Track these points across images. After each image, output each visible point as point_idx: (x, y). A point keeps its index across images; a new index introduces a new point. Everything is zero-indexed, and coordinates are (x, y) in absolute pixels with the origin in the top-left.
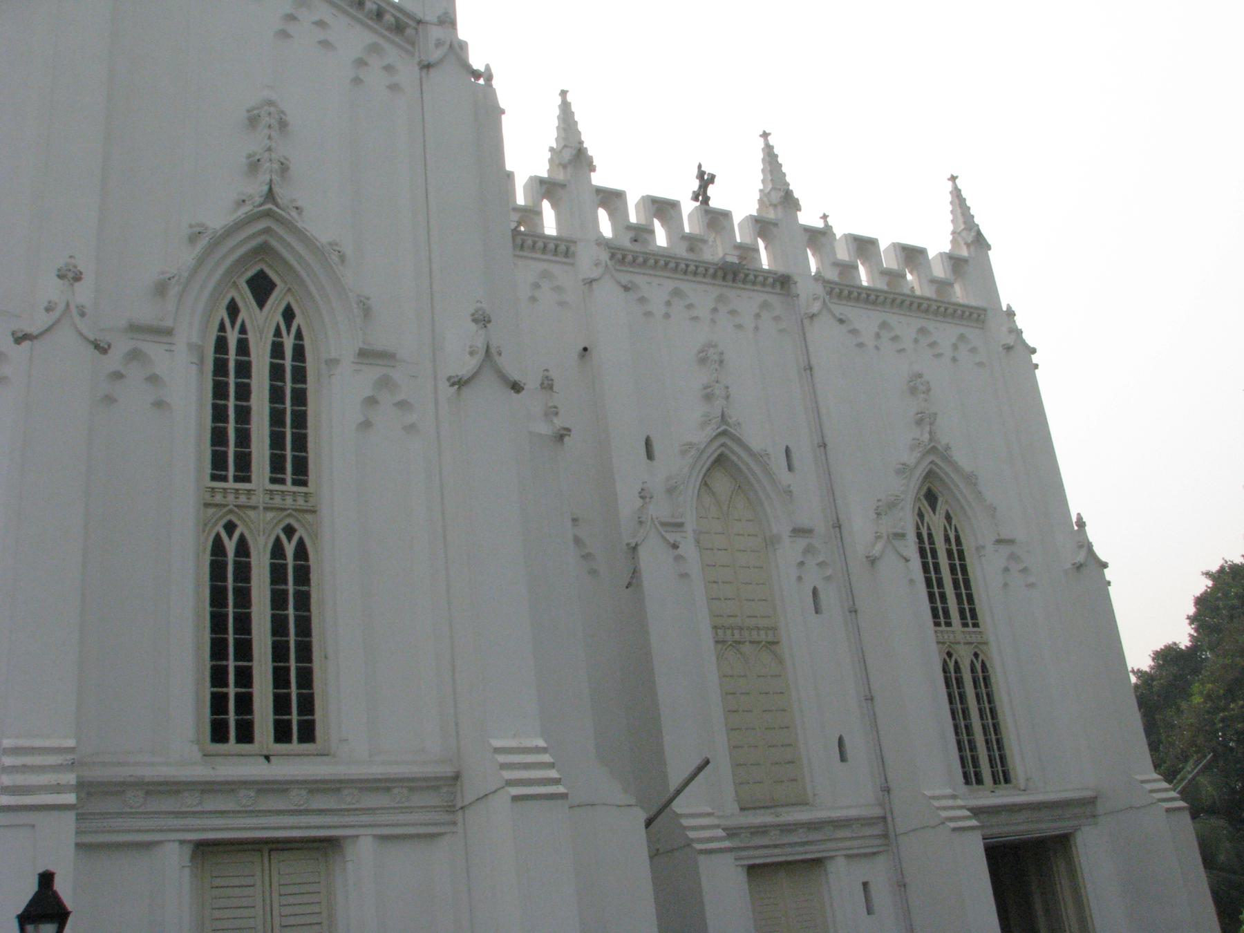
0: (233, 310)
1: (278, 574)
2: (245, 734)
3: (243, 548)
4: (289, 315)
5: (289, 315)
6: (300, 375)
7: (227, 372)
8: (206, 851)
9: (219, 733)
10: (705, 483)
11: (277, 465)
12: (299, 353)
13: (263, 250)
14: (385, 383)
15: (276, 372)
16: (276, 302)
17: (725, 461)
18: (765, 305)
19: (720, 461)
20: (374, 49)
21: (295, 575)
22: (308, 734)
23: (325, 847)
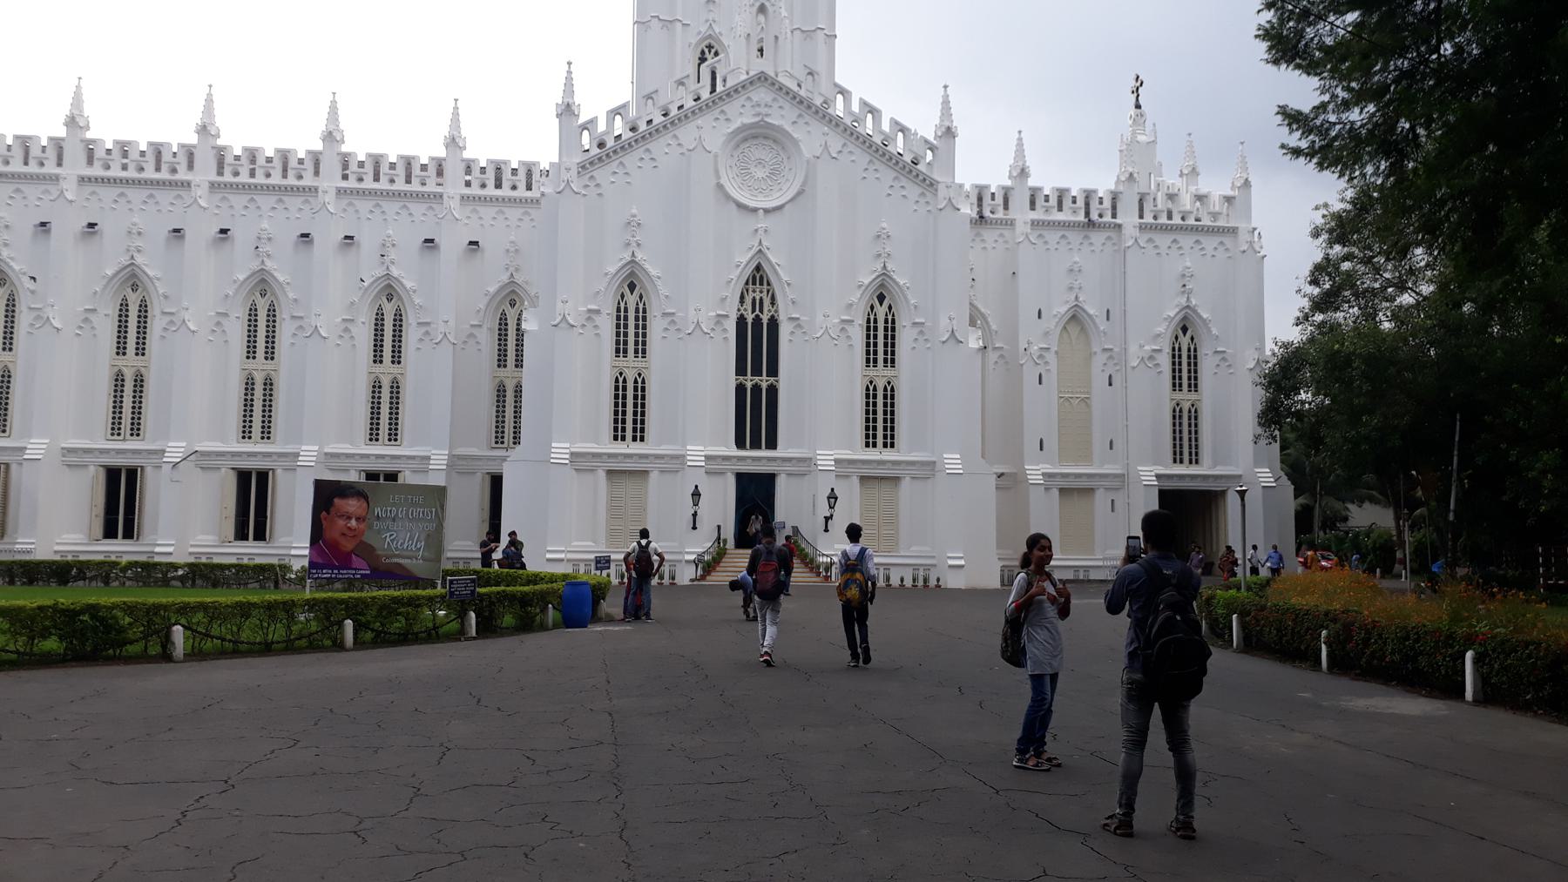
0: (872, 307)
1: (885, 397)
2: (875, 445)
3: (875, 389)
4: (890, 308)
5: (890, 308)
6: (893, 329)
7: (870, 328)
8: (863, 479)
11: (885, 361)
12: (893, 321)
13: (882, 285)
14: (921, 332)
15: (886, 329)
17: (1076, 318)
18: (1109, 238)
19: (1074, 317)
21: (890, 394)
22: (892, 446)
23: (896, 480)
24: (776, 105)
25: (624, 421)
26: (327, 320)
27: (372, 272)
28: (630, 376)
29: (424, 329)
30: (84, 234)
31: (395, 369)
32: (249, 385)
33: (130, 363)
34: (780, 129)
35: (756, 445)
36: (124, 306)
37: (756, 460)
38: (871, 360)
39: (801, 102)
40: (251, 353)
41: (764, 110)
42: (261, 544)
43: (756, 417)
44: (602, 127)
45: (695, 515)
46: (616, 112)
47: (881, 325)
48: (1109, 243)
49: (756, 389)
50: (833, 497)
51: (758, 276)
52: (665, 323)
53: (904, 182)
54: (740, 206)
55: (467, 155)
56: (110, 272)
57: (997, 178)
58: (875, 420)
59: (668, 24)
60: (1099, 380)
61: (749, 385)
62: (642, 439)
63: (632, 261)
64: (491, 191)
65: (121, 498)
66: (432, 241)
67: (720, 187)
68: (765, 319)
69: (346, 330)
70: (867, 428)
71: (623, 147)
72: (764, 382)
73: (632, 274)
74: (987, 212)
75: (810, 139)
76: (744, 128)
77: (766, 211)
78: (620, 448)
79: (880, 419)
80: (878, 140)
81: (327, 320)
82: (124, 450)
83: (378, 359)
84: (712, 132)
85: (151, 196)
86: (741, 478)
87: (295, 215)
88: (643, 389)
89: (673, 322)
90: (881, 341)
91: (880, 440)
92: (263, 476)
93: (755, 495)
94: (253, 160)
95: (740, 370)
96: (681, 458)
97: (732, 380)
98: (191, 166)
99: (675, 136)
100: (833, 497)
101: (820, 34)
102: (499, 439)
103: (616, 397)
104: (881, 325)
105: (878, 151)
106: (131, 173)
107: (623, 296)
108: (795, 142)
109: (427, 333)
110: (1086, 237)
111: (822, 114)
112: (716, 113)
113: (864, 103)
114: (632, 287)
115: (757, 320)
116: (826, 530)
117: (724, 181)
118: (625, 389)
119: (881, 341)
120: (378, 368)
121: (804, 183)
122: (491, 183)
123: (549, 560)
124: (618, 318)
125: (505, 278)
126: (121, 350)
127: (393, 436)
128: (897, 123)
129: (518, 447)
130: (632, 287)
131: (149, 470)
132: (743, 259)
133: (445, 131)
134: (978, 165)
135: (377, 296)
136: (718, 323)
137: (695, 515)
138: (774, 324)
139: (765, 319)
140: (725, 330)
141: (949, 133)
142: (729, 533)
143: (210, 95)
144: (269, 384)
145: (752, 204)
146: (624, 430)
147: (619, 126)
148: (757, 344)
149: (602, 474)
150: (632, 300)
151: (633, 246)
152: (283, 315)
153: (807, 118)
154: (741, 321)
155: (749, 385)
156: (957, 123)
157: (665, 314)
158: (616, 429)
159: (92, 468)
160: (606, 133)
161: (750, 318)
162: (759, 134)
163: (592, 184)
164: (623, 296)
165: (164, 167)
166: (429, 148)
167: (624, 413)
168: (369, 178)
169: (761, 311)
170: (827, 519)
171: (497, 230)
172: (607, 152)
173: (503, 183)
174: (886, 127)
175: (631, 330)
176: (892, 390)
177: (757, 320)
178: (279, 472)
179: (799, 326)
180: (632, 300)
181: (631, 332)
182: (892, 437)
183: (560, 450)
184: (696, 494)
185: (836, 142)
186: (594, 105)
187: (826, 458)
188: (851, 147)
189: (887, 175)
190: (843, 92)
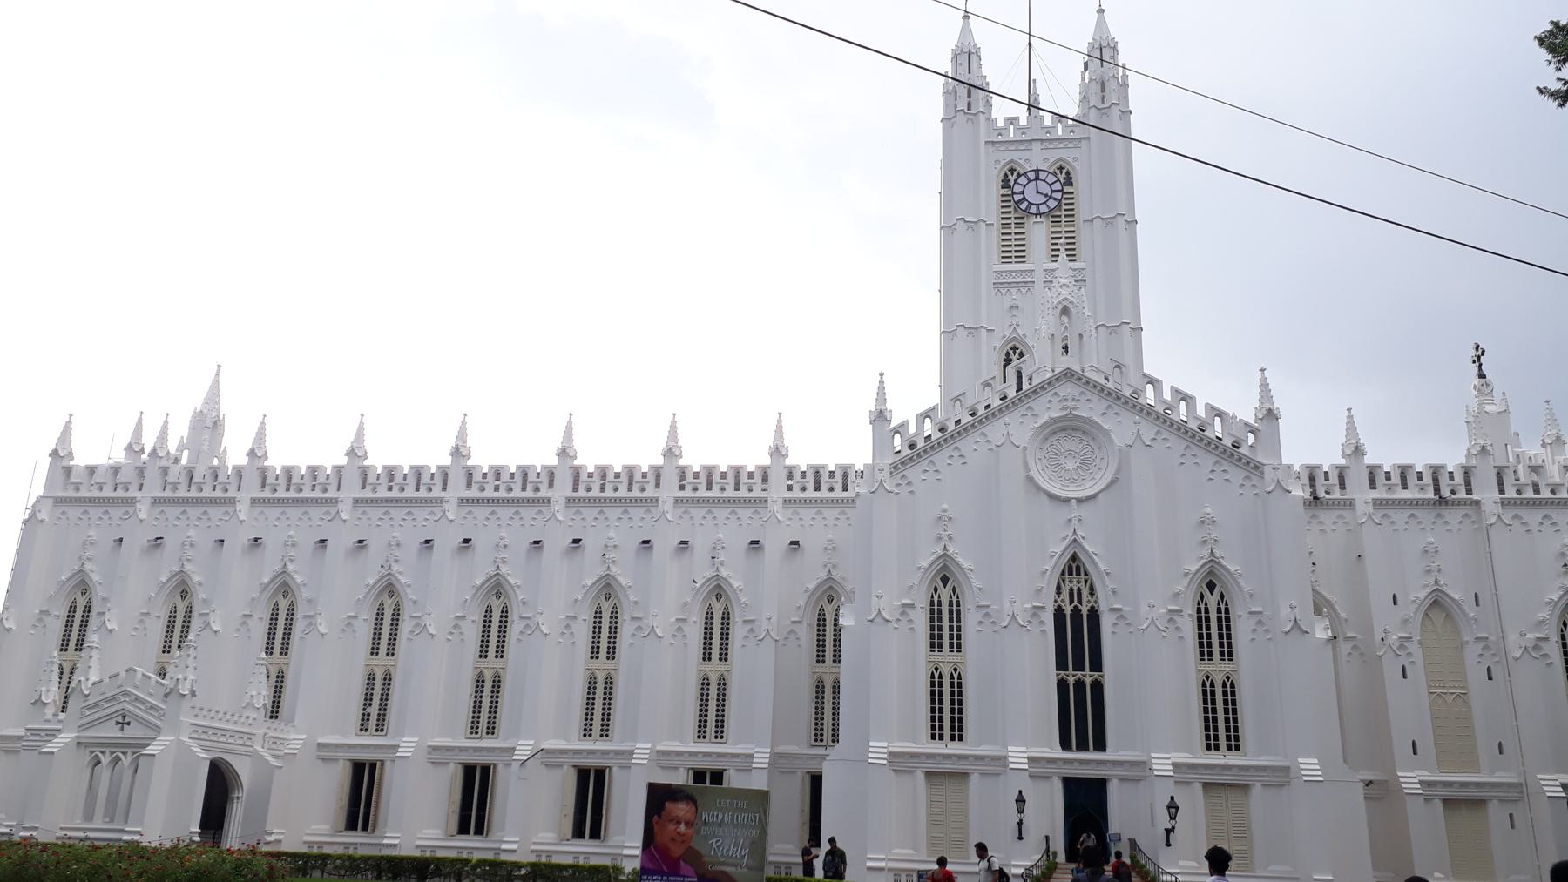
0: (1202, 596)
1: (1225, 693)
3: (1212, 685)
4: (1222, 596)
5: (1222, 596)
6: (1228, 619)
7: (1202, 618)
8: (1207, 786)
9: (1208, 747)
10: (1426, 614)
11: (1222, 653)
12: (1227, 611)
14: (1260, 622)
15: (1219, 619)
16: (1217, 591)
17: (1438, 603)
19: (1435, 603)
20: (1247, 477)
22: (1237, 748)
23: (1244, 787)
24: (1083, 398)
25: (941, 719)
26: (662, 622)
27: (703, 573)
28: (946, 671)
29: (749, 627)
30: (461, 548)
31: (722, 666)
32: (592, 684)
33: (490, 665)
34: (1089, 421)
35: (1083, 746)
36: (488, 612)
37: (1085, 762)
38: (1205, 653)
39: (1110, 394)
40: (595, 654)
41: (1070, 404)
42: (596, 842)
43: (1082, 716)
44: (912, 429)
45: (1020, 823)
46: (926, 415)
47: (1213, 615)
48: (1467, 521)
49: (1080, 685)
50: (1173, 807)
51: (1074, 566)
52: (979, 615)
53: (1226, 466)
54: (1052, 496)
55: (788, 462)
56: (478, 582)
57: (1329, 457)
58: (1215, 720)
59: (973, 331)
60: (1476, 674)
61: (1071, 680)
62: (961, 739)
63: (945, 555)
64: (811, 493)
65: (475, 794)
66: (757, 542)
67: (1030, 479)
68: (1084, 610)
69: (680, 629)
70: (1207, 728)
71: (932, 446)
72: (1088, 677)
73: (945, 567)
74: (1321, 492)
75: (1121, 429)
76: (1052, 421)
77: (1079, 501)
78: (938, 748)
79: (1221, 717)
80: (1193, 425)
81: (662, 622)
82: (481, 747)
83: (707, 657)
84: (1020, 428)
85: (517, 513)
86: (1067, 781)
87: (529, 524)
88: (960, 685)
89: (987, 615)
90: (1215, 632)
91: (1223, 742)
92: (601, 774)
93: (1085, 803)
94: (604, 477)
95: (1061, 664)
96: (1002, 760)
97: (1053, 676)
98: (551, 485)
99: (983, 434)
100: (1173, 807)
101: (1126, 328)
102: (818, 736)
103: (933, 693)
104: (1213, 615)
105: (1196, 436)
106: (502, 494)
107: (936, 590)
108: (1106, 432)
109: (752, 630)
110: (1439, 515)
111: (1132, 404)
112: (1023, 410)
113: (1175, 391)
114: (945, 580)
115: (1076, 612)
116: (1168, 845)
117: (1034, 473)
118: (941, 684)
119: (1215, 632)
120: (707, 666)
121: (1117, 472)
122: (810, 486)
123: (870, 869)
124: (932, 612)
125: (823, 575)
126: (483, 653)
127: (720, 734)
128: (1213, 408)
129: (837, 746)
130: (945, 580)
131: (500, 768)
132: (1059, 549)
133: (558, 443)
134: (1308, 444)
135: (707, 597)
136: (1034, 615)
137: (1020, 823)
138: (1094, 615)
139: (1084, 610)
140: (1042, 622)
141: (1271, 415)
142: (1059, 845)
143: (570, 422)
144: (609, 683)
145: (1063, 494)
146: (941, 728)
147: (928, 427)
148: (1078, 637)
149: (920, 776)
150: (945, 593)
151: (945, 541)
152: (624, 617)
153: (1117, 409)
154: (1059, 613)
155: (1071, 680)
156: (1279, 404)
157: (979, 607)
158: (933, 728)
159: (452, 765)
160: (916, 435)
161: (1068, 609)
162: (1069, 426)
163: (903, 482)
164: (936, 590)
165: (529, 487)
166: (755, 457)
167: (941, 710)
168: (517, 487)
169: (1080, 601)
170: (1169, 831)
171: (817, 531)
172: (918, 452)
173: (823, 487)
174: (1201, 412)
175: (945, 624)
176: (1232, 685)
177: (1076, 612)
178: (615, 769)
179: (1122, 617)
180: (945, 593)
181: (945, 626)
182: (1237, 739)
183: (878, 750)
184: (1020, 800)
185: (1148, 431)
186: (904, 411)
187: (1162, 762)
188: (1166, 435)
189: (1207, 460)
190: (1152, 381)
